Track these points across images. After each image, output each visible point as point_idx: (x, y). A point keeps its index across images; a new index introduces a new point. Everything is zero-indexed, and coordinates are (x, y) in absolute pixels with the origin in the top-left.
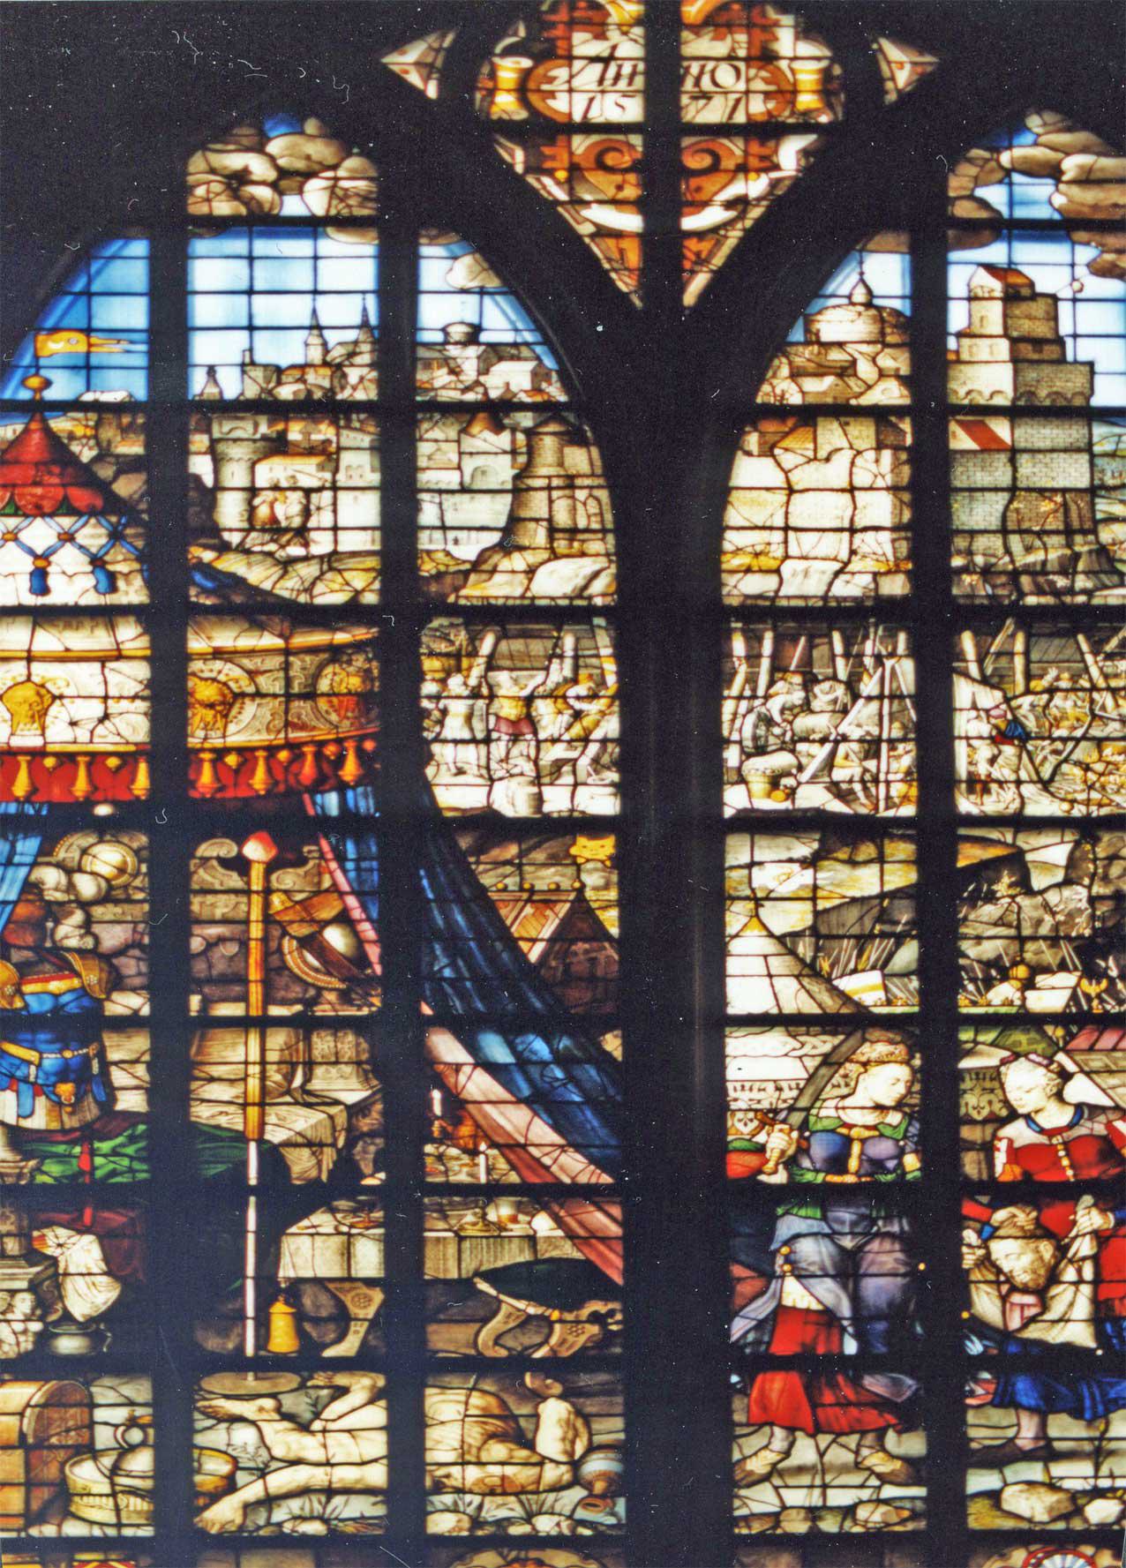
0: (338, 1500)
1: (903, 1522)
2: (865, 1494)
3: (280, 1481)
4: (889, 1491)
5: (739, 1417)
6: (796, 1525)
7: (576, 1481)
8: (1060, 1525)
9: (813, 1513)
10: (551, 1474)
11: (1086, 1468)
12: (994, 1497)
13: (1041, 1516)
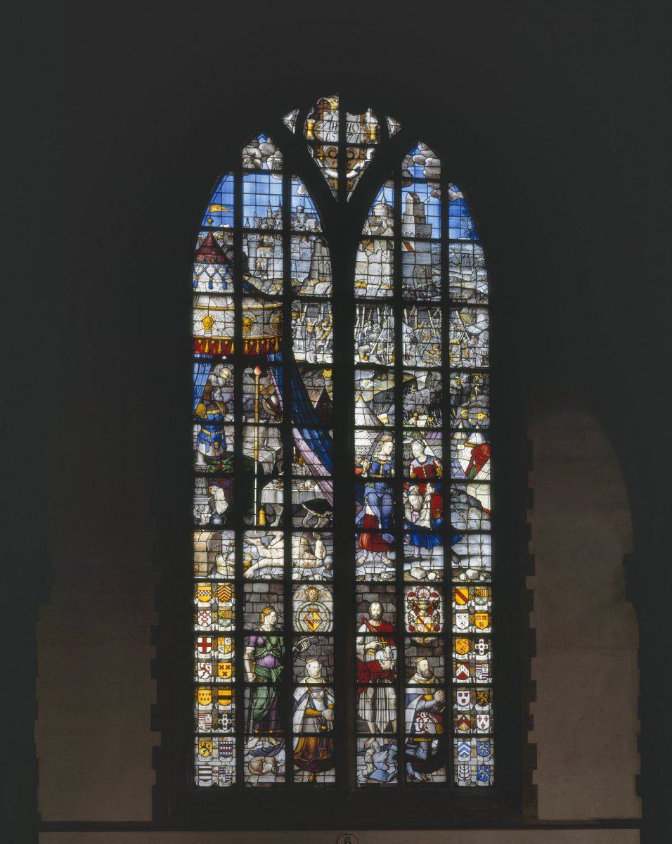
0: (274, 569)
1: (391, 578)
2: (383, 570)
3: (262, 563)
4: (388, 569)
5: (357, 547)
6: (369, 579)
7: (323, 565)
8: (423, 580)
9: (372, 575)
10: (319, 562)
11: (427, 564)
12: (409, 571)
13: (419, 578)
